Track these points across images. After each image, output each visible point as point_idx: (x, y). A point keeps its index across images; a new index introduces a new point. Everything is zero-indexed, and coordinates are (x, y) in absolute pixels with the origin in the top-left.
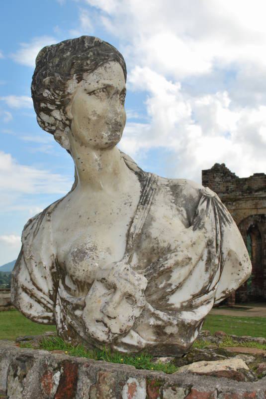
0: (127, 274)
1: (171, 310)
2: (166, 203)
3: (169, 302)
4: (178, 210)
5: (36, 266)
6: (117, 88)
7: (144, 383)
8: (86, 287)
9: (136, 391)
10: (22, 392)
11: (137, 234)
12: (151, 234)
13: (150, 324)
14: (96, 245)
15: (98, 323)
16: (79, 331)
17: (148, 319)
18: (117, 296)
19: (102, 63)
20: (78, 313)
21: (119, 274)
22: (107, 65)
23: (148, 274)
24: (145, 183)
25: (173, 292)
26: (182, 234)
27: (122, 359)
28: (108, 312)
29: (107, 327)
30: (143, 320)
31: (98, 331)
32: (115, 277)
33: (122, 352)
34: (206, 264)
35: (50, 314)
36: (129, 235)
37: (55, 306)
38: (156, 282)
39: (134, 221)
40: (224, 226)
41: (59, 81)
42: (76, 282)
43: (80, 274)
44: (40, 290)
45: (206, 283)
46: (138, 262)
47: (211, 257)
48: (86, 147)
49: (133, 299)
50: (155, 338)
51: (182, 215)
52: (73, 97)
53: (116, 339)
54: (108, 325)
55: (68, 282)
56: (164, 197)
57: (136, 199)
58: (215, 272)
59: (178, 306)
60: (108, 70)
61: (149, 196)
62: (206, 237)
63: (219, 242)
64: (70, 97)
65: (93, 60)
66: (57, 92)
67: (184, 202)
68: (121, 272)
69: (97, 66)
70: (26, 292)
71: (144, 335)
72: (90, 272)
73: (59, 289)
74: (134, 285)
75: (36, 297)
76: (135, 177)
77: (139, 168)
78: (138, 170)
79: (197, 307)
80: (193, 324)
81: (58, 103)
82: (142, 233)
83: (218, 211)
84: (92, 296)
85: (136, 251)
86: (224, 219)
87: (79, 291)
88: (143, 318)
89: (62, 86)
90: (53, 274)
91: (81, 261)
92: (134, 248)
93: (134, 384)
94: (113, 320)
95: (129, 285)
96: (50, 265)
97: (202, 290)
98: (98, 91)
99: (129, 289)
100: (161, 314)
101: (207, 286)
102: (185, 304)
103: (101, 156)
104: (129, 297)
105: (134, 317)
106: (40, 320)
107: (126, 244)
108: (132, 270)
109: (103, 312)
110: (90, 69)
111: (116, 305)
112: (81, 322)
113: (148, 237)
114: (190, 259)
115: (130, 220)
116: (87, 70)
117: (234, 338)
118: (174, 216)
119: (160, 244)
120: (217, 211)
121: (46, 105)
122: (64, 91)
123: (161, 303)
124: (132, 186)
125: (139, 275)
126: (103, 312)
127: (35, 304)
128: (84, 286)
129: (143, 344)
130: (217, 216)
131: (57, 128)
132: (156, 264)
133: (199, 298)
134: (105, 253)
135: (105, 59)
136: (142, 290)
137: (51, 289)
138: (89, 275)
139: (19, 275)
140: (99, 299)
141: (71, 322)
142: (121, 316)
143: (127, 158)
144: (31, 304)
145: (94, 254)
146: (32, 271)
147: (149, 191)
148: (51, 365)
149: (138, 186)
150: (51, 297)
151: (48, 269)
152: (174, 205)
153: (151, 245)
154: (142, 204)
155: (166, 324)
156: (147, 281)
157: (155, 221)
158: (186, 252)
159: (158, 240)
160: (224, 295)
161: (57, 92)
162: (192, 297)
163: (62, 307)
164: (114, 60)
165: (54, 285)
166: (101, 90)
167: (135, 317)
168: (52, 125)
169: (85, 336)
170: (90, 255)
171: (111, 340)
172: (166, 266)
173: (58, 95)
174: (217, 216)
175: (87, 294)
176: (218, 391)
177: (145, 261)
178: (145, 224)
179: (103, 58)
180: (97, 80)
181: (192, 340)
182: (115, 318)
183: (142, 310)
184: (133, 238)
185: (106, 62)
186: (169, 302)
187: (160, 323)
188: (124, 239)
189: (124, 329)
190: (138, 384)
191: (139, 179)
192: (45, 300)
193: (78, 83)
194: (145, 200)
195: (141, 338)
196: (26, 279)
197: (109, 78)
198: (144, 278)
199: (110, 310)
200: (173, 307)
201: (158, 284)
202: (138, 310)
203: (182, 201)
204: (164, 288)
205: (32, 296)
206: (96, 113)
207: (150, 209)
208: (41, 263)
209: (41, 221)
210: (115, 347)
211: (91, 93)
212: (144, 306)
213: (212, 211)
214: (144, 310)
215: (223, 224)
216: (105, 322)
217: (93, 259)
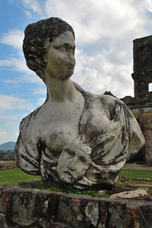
0: (80, 146)
1: (104, 165)
2: (99, 108)
3: (103, 161)
4: (105, 111)
5: (29, 143)
6: (71, 45)
7: (97, 205)
8: (58, 154)
9: (93, 209)
10: (27, 212)
11: (84, 125)
12: (92, 124)
13: (94, 173)
15: (66, 173)
16: (55, 178)
17: (92, 170)
18: (76, 158)
19: (63, 31)
20: (54, 168)
21: (76, 146)
22: (66, 33)
24: (86, 97)
25: (105, 155)
26: (109, 123)
27: (80, 192)
28: (71, 167)
29: (70, 175)
31: (66, 178)
32: (74, 148)
33: (79, 189)
34: (122, 139)
35: (37, 170)
36: (80, 125)
37: (40, 165)
38: (96, 150)
39: (82, 117)
40: (130, 119)
41: (40, 41)
42: (52, 151)
43: (54, 147)
44: (32, 156)
45: (122, 150)
46: (85, 139)
47: (124, 136)
48: (54, 78)
49: (84, 159)
50: (96, 180)
51: (108, 114)
52: (47, 51)
54: (71, 174)
55: (47, 151)
56: (97, 105)
57: (82, 106)
58: (126, 144)
59: (107, 162)
61: (89, 104)
62: (121, 125)
63: (128, 128)
65: (57, 30)
66: (39, 48)
67: (108, 107)
69: (60, 33)
70: (24, 158)
71: (91, 179)
72: (60, 146)
73: (42, 156)
74: (84, 152)
75: (29, 161)
76: (80, 94)
77: (82, 89)
78: (82, 91)
79: (117, 163)
80: (116, 172)
81: (39, 54)
82: (87, 124)
83: (126, 111)
84: (62, 159)
85: (84, 134)
86: (130, 115)
87: (54, 156)
89: (42, 44)
90: (38, 148)
91: (55, 140)
92: (83, 132)
93: (92, 206)
94: (74, 171)
95: (82, 152)
96: (37, 143)
97: (120, 154)
98: (61, 47)
99: (82, 154)
100: (99, 167)
101: (123, 151)
102: (111, 162)
103: (62, 83)
104: (82, 159)
105: (85, 170)
106: (32, 173)
107: (78, 130)
108: (83, 144)
109: (68, 167)
112: (55, 173)
113: (91, 126)
114: (114, 137)
115: (80, 117)
116: (55, 36)
117: (133, 179)
118: (103, 114)
119: (97, 129)
120: (125, 111)
121: (32, 55)
122: (42, 47)
123: (98, 161)
124: (79, 98)
125: (87, 147)
126: (68, 167)
127: (29, 164)
128: (57, 153)
129: (90, 184)
130: (126, 114)
131: (38, 68)
133: (119, 158)
134: (68, 135)
135: (64, 30)
136: (89, 155)
137: (37, 156)
138: (59, 147)
139: (19, 149)
141: (50, 173)
142: (78, 170)
143: (76, 84)
144: (27, 165)
145: (62, 136)
146: (27, 146)
147: (89, 101)
148: (42, 197)
149: (83, 98)
150: (37, 160)
151: (35, 145)
152: (103, 108)
153: (92, 130)
154: (86, 108)
155: (102, 172)
156: (91, 150)
157: (93, 117)
158: (111, 134)
159: (96, 128)
160: (130, 156)
161: (39, 48)
162: (115, 157)
163: (44, 165)
164: (69, 30)
165: (39, 153)
168: (35, 67)
172: (101, 141)
173: (39, 49)
174: (126, 114)
175: (58, 158)
176: (140, 207)
177: (89, 139)
178: (88, 119)
179: (63, 29)
181: (116, 180)
182: (75, 170)
183: (89, 165)
184: (82, 126)
185: (65, 31)
186: (103, 161)
187: (99, 172)
188: (77, 127)
190: (94, 205)
191: (83, 95)
192: (34, 162)
193: (50, 43)
194: (87, 106)
196: (23, 151)
197: (67, 40)
198: (90, 148)
199: (72, 165)
200: (105, 163)
201: (97, 151)
203: (107, 106)
204: (100, 153)
205: (27, 160)
206: (60, 59)
207: (90, 111)
208: (31, 142)
209: (30, 119)
210: (75, 186)
211: (57, 48)
212: (90, 163)
213: (123, 112)
214: (90, 165)
215: (129, 118)
217: (61, 138)
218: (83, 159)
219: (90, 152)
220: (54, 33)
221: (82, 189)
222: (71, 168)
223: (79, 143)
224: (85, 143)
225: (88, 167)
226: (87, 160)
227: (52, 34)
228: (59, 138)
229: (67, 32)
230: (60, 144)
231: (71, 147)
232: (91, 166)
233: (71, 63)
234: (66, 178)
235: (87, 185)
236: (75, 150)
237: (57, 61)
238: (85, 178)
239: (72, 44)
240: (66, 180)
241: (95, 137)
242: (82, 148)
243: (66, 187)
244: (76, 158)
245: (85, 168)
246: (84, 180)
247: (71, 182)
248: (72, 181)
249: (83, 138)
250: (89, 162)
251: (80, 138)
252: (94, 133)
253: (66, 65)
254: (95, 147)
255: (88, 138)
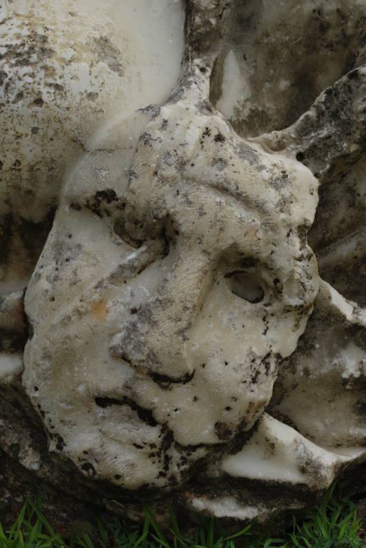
0: (220, 162)
8: (17, 242)
13: (345, 375)
14: (40, 31)
15: (107, 411)
16: (16, 447)
17: (332, 354)
18: (188, 273)
21: (182, 164)
23: (314, 146)
28: (152, 356)
29: (152, 422)
30: (311, 364)
31: (112, 448)
33: (231, 524)
38: (349, 180)
46: (248, 93)
53: (201, 465)
54: (160, 416)
68: (190, 149)
72: (31, 169)
84: (63, 286)
85: (236, 41)
88: (310, 355)
92: (226, 29)
95: (237, 211)
99: (240, 226)
104: (244, 273)
105: (273, 362)
107: (178, 18)
108: (238, 140)
109: (125, 358)
111: (186, 316)
112: (17, 404)
125: (277, 158)
126: (125, 358)
129: (323, 472)
132: (342, 96)
138: (25, 185)
140: (96, 297)
142: (215, 367)
145: (42, 73)
156: (316, 183)
167: (278, 356)
169: (46, 468)
170: (19, 85)
171: (179, 478)
175: (28, 270)
177: (284, 84)
182: (188, 378)
183: (304, 323)
189: (238, 423)
195: (305, 440)
198: (300, 166)
199: (159, 338)
202: (289, 322)
210: (199, 503)
212: (315, 302)
214: (311, 319)
216: (143, 403)
217: (39, 102)
218: (251, 270)
219: (305, 209)
221: (254, 522)
222: (154, 367)
223: (207, 132)
224: (249, 124)
225: (301, 331)
226: (291, 279)
228: (20, 95)
230: (30, 151)
231: (131, 174)
232: (318, 318)
234: (112, 448)
235: (300, 485)
236: (173, 204)
238: (278, 430)
240: (121, 468)
241: (334, 68)
242: (239, 172)
243: (124, 519)
244: (188, 273)
245: (275, 350)
246: (271, 448)
247: (161, 474)
248: (166, 468)
249: (224, 87)
250: (301, 295)
251: (201, 88)
252: (324, 28)
254: (346, 156)
255: (271, 79)
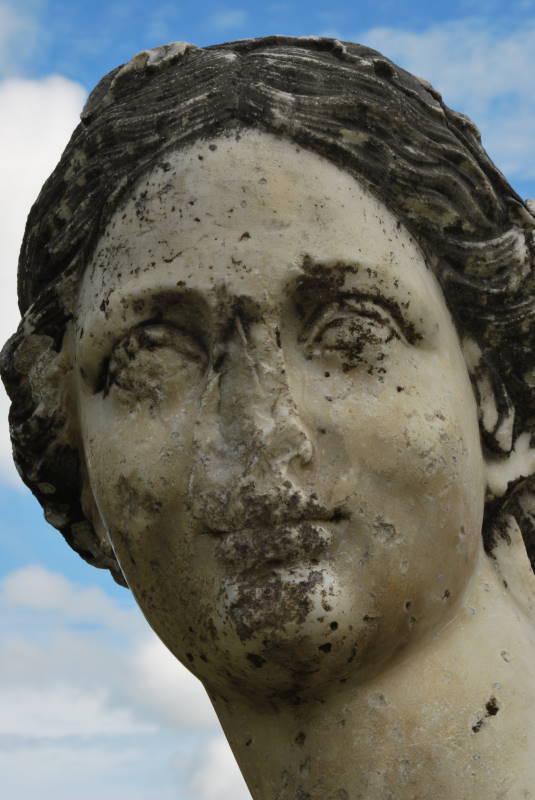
6: (222, 290)
19: (124, 181)
22: (158, 178)
52: (77, 435)
60: (154, 205)
64: (63, 436)
65: (79, 194)
98: (121, 352)
103: (301, 738)
110: (75, 250)
164: (212, 131)
166: (134, 341)
179: (129, 149)
180: (102, 298)
185: (150, 168)
193: (57, 348)
197: (161, 251)
211: (103, 379)
220: (55, 233)
227: (48, 256)
229: (172, 159)
233: (249, 502)
237: (122, 525)
239: (225, 275)
253: (219, 534)
